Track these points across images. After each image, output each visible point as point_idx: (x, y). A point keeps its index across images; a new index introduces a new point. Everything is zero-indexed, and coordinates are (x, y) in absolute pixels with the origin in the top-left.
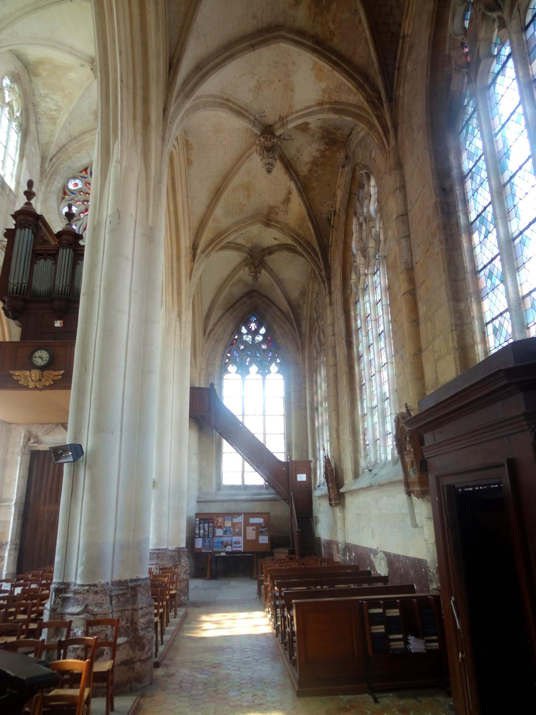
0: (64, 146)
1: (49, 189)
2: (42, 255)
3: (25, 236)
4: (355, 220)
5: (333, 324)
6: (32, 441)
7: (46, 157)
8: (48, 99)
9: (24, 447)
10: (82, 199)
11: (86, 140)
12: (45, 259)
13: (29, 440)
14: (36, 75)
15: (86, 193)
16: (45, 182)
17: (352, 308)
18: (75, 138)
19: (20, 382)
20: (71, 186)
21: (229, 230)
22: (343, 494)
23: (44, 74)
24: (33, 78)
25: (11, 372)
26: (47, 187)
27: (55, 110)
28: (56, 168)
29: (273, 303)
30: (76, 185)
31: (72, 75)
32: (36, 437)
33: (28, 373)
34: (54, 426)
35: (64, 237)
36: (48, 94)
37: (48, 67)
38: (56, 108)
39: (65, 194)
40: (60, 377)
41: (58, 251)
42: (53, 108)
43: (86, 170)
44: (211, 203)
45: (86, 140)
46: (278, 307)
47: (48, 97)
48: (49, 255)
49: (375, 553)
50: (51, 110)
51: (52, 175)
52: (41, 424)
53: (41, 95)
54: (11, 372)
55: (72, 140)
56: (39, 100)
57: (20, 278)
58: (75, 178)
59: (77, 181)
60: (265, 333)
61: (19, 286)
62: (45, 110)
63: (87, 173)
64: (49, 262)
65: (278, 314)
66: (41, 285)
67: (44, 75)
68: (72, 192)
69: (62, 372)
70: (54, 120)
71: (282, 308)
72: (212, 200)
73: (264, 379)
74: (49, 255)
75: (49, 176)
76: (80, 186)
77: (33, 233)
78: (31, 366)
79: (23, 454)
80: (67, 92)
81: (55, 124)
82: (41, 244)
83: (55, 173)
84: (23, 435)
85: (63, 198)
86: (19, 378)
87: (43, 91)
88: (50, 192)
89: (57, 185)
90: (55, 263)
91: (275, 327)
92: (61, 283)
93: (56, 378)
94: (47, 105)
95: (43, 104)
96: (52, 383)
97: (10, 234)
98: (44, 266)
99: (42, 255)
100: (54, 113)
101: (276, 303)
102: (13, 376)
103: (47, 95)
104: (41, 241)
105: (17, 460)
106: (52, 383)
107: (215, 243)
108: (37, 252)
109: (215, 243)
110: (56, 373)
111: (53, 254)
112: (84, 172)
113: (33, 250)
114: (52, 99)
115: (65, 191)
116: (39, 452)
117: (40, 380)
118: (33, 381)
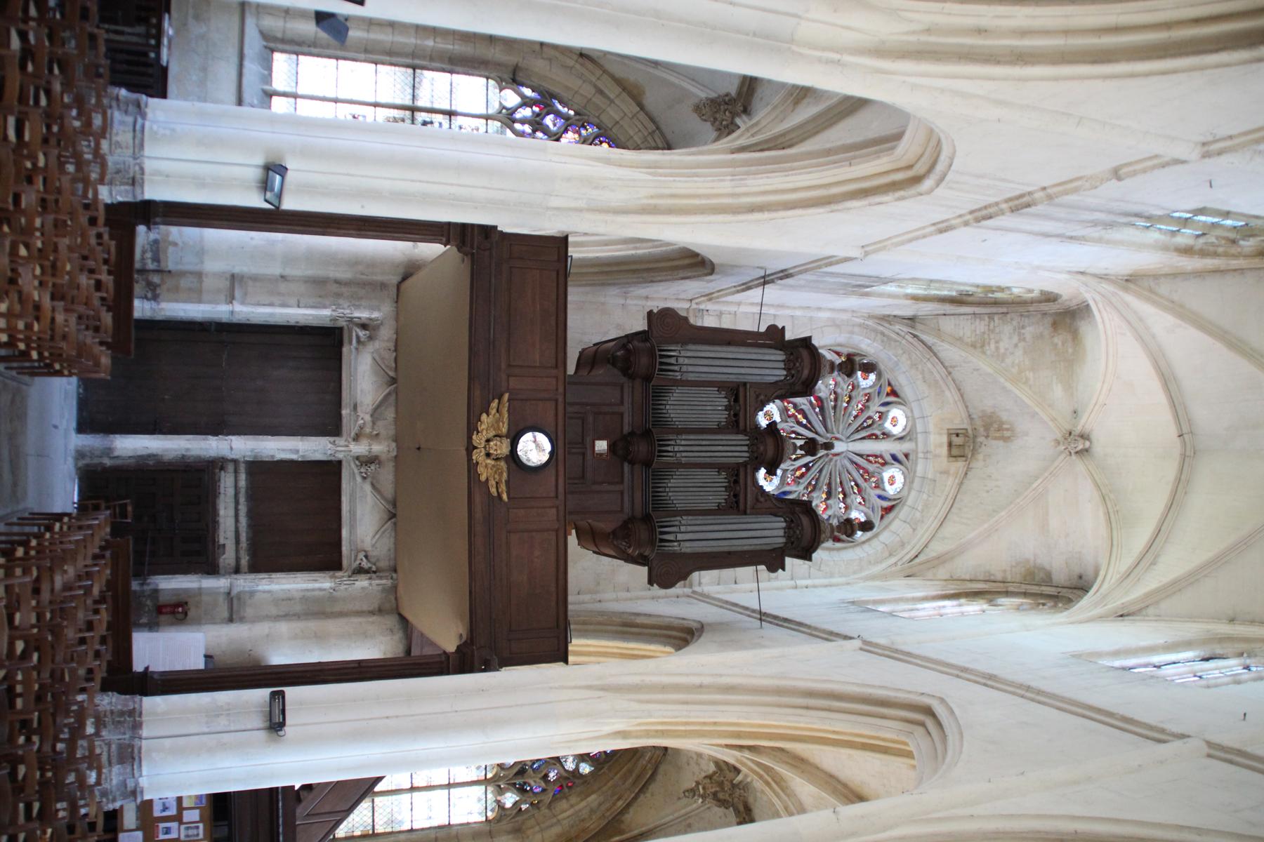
1: (856, 329)
2: (736, 400)
3: (772, 367)
6: (362, 333)
7: (913, 327)
8: (1015, 339)
9: (351, 320)
10: (839, 390)
11: (947, 393)
12: (728, 408)
13: (364, 326)
14: (1055, 325)
15: (850, 397)
16: (870, 323)
18: (950, 373)
19: (484, 416)
21: (788, 796)
23: (1058, 340)
24: (1048, 320)
25: (506, 396)
26: (860, 325)
27: (997, 348)
28: (896, 341)
29: (642, 790)
31: (1058, 391)
32: (371, 338)
33: (504, 430)
34: (392, 374)
35: (770, 442)
36: (1024, 340)
37: (1070, 350)
38: (1002, 351)
40: (493, 491)
41: (744, 432)
42: (1002, 345)
43: (894, 393)
44: (839, 781)
45: (947, 393)
46: (635, 798)
47: (1020, 340)
48: (736, 415)
50: (997, 342)
51: (883, 334)
52: (396, 346)
53: (1023, 327)
54: (506, 396)
55: (945, 367)
56: (1015, 323)
57: (691, 369)
60: (581, 775)
61: (676, 368)
62: (997, 330)
63: (888, 395)
64: (722, 417)
65: (620, 803)
66: (679, 407)
67: (1056, 340)
69: (505, 497)
70: (978, 345)
71: (632, 810)
72: (845, 786)
73: (485, 782)
74: (736, 415)
75: (881, 328)
77: (776, 382)
79: (334, 320)
80: (1030, 375)
81: (973, 346)
82: (758, 396)
84: (375, 315)
85: (838, 354)
86: (493, 411)
87: (1029, 331)
88: (852, 333)
90: (719, 430)
91: (593, 799)
92: (682, 448)
93: (492, 483)
94: (1006, 334)
95: (1007, 329)
96: (483, 478)
97: (774, 336)
98: (715, 408)
99: (736, 400)
100: (993, 346)
101: (642, 796)
102: (496, 401)
103: (1022, 339)
104: (762, 397)
105: (325, 307)
106: (483, 478)
107: (762, 772)
108: (741, 389)
109: (762, 772)
110: (503, 487)
111: (737, 422)
112: (888, 389)
113: (745, 384)
114: (1016, 346)
117: (488, 455)
118: (488, 441)
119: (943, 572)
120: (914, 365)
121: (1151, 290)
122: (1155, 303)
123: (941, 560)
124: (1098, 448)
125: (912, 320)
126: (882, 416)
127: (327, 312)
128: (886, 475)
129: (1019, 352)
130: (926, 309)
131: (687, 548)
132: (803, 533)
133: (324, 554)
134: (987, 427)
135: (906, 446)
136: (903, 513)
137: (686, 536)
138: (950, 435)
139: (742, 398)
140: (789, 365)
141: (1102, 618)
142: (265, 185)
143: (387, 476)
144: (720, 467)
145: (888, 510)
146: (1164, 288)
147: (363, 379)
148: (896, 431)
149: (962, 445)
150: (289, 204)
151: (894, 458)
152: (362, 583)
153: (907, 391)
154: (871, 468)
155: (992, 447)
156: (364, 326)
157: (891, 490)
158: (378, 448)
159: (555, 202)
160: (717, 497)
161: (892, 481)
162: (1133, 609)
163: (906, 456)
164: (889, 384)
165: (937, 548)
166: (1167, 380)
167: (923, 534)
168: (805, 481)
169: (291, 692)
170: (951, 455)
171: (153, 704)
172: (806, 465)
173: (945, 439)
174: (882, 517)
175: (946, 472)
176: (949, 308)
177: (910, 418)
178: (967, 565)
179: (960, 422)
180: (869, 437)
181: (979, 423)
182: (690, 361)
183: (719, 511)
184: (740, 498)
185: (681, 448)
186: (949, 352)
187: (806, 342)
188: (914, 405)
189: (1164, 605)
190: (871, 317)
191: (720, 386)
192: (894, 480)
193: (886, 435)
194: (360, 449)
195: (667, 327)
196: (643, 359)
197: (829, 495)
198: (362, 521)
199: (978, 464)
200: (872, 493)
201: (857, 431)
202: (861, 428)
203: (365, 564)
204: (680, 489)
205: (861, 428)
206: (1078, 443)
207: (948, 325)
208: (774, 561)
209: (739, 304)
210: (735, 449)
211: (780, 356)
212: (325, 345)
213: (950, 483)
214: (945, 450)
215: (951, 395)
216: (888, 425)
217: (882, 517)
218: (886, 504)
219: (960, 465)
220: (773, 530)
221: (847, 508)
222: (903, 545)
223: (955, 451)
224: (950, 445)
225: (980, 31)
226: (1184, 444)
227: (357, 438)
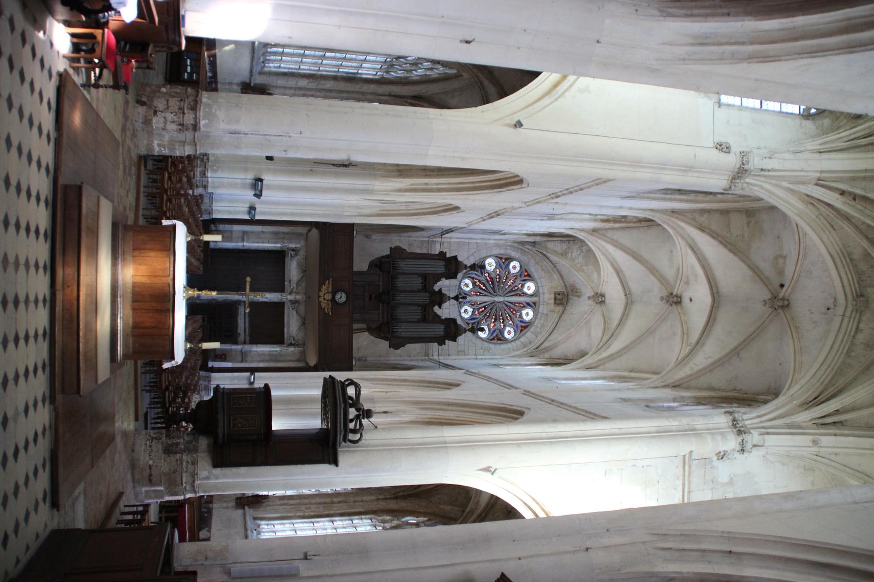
0: (548, 258)
4: (426, 519)
5: (362, 501)
17: (367, 516)
20: (512, 264)
22: (244, 508)
30: (514, 268)
32: (296, 255)
39: (506, 259)
42: (574, 254)
43: (529, 275)
49: (209, 531)
58: (521, 267)
59: (518, 269)
68: (508, 265)
70: (564, 254)
76: (513, 271)
78: (334, 294)
80: (585, 268)
81: (562, 255)
83: (523, 252)
84: (298, 246)
85: (501, 258)
89: (513, 254)
90: (419, 291)
97: (442, 254)
98: (417, 283)
115: (509, 259)
116: (284, 257)
119: (547, 355)
120: (537, 263)
121: (604, 236)
122: (605, 241)
123: (547, 349)
124: (607, 301)
125: (534, 244)
126: (523, 286)
127: (279, 245)
128: (524, 312)
129: (581, 258)
130: (538, 239)
131: (403, 335)
132: (451, 330)
133: (277, 338)
134: (572, 291)
135: (534, 299)
136: (532, 329)
137: (403, 330)
138: (555, 294)
139: (428, 280)
140: (446, 267)
141: (578, 369)
142: (249, 213)
143: (302, 308)
144: (419, 305)
145: (525, 327)
146: (609, 234)
147: (293, 270)
148: (530, 292)
149: (563, 299)
150: (257, 217)
151: (528, 304)
152: (292, 349)
153: (535, 275)
154: (516, 308)
155: (574, 299)
156: (293, 250)
157: (526, 319)
158: (298, 297)
159: (346, 214)
160: (418, 316)
161: (527, 314)
162: (593, 365)
163: (535, 304)
164: (526, 271)
165: (546, 344)
166: (619, 272)
167: (541, 338)
168: (484, 314)
169: (256, 374)
170: (555, 303)
171: (214, 375)
172: (484, 307)
173: (553, 296)
174: (521, 331)
175: (554, 311)
176: (545, 239)
177: (537, 287)
178: (557, 352)
179: (560, 288)
180: (516, 295)
181: (569, 289)
182: (404, 266)
183: (418, 321)
184: (428, 316)
185: (401, 298)
186: (553, 257)
187: (455, 258)
188: (538, 281)
189: (607, 365)
190: (514, 242)
191: (419, 275)
192: (528, 314)
193: (525, 294)
194: (291, 297)
195: (397, 253)
196: (388, 265)
197: (496, 320)
198: (292, 325)
199: (568, 308)
200: (517, 320)
201: (510, 292)
202: (511, 291)
203: (293, 342)
204: (401, 313)
205: (511, 291)
206: (600, 298)
207: (550, 245)
208: (441, 342)
209: (451, 238)
210: (424, 298)
211: (443, 263)
212: (278, 258)
213: (555, 316)
214: (552, 301)
215: (556, 276)
216: (525, 290)
217: (521, 331)
218: (523, 325)
219: (561, 308)
220: (440, 330)
221: (504, 326)
222: (531, 343)
223: (558, 302)
224: (555, 299)
225: (426, 184)
226: (627, 298)
227: (290, 293)
